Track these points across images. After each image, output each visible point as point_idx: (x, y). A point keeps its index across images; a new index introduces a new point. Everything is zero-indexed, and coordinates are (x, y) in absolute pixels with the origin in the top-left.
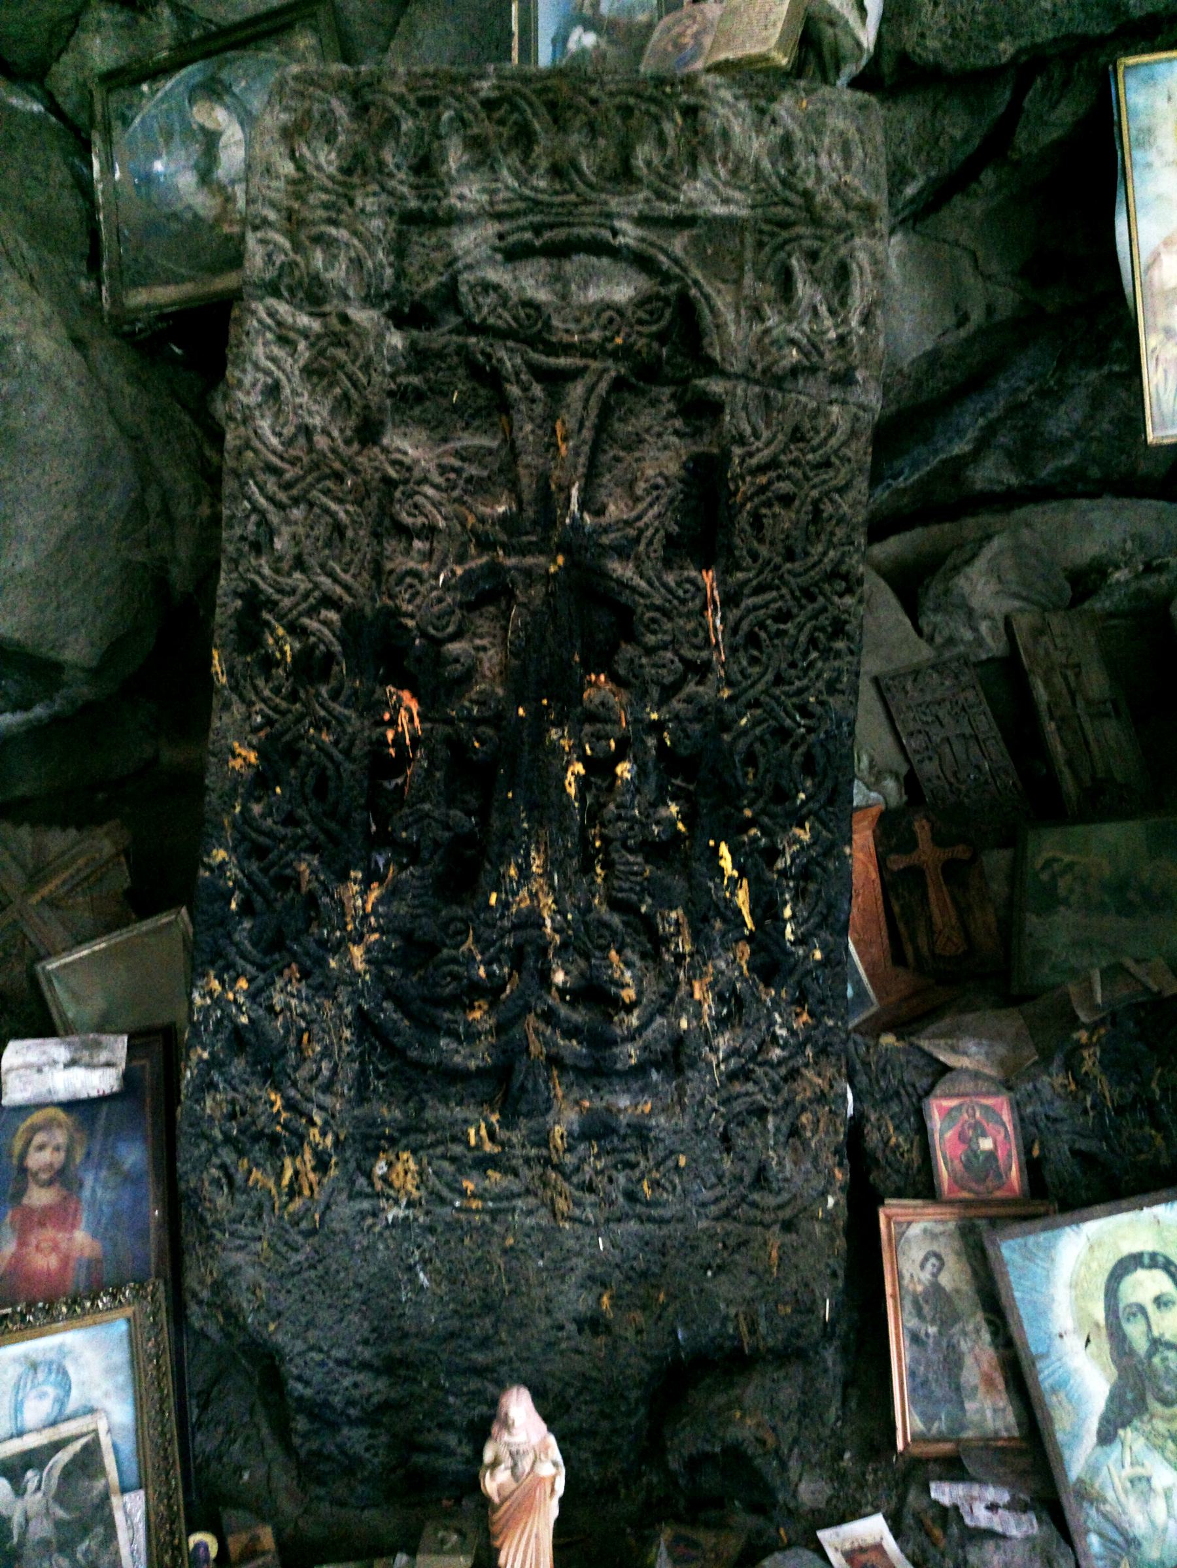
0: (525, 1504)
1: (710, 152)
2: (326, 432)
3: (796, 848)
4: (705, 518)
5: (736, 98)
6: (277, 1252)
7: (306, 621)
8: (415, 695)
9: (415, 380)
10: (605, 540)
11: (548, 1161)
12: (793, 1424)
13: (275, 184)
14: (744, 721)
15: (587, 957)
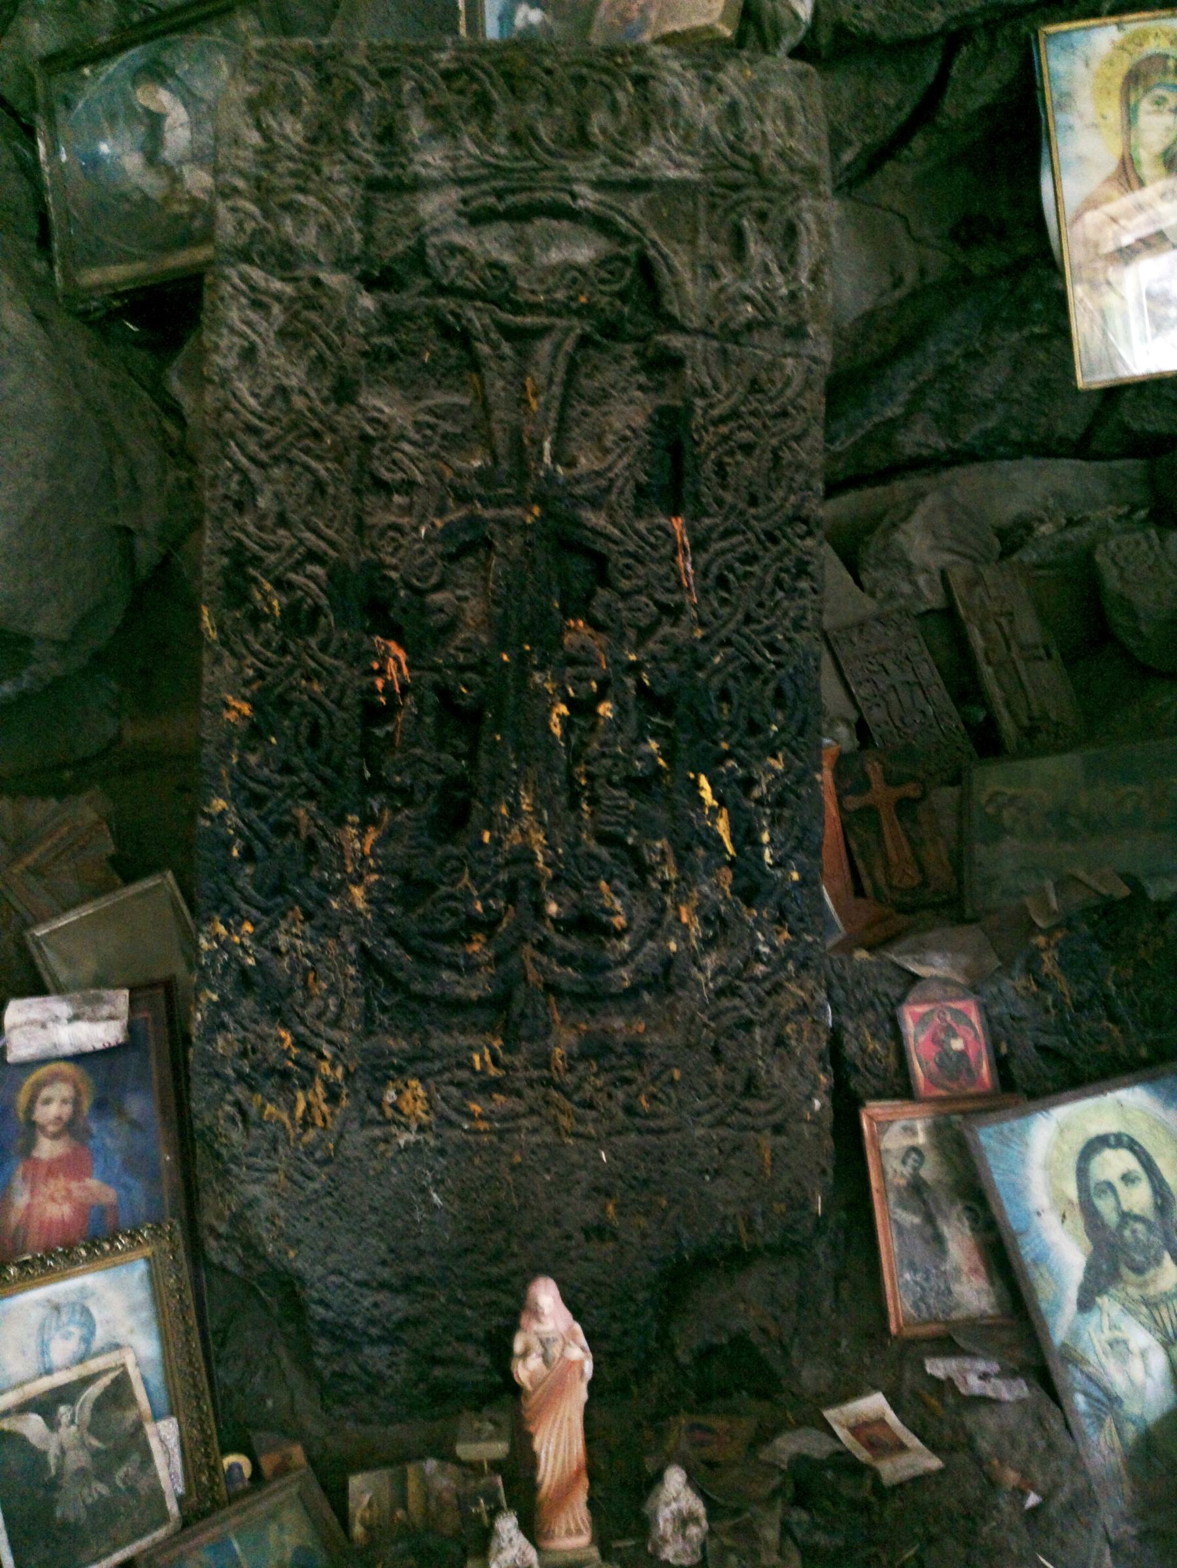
0: (556, 1388)
1: (661, 119)
2: (303, 392)
3: (771, 777)
4: (673, 468)
5: (684, 67)
6: (294, 1182)
7: (292, 576)
8: (401, 644)
9: (388, 340)
10: (578, 491)
11: (549, 1083)
12: (793, 1315)
13: (241, 153)
14: (717, 660)
15: (577, 888)
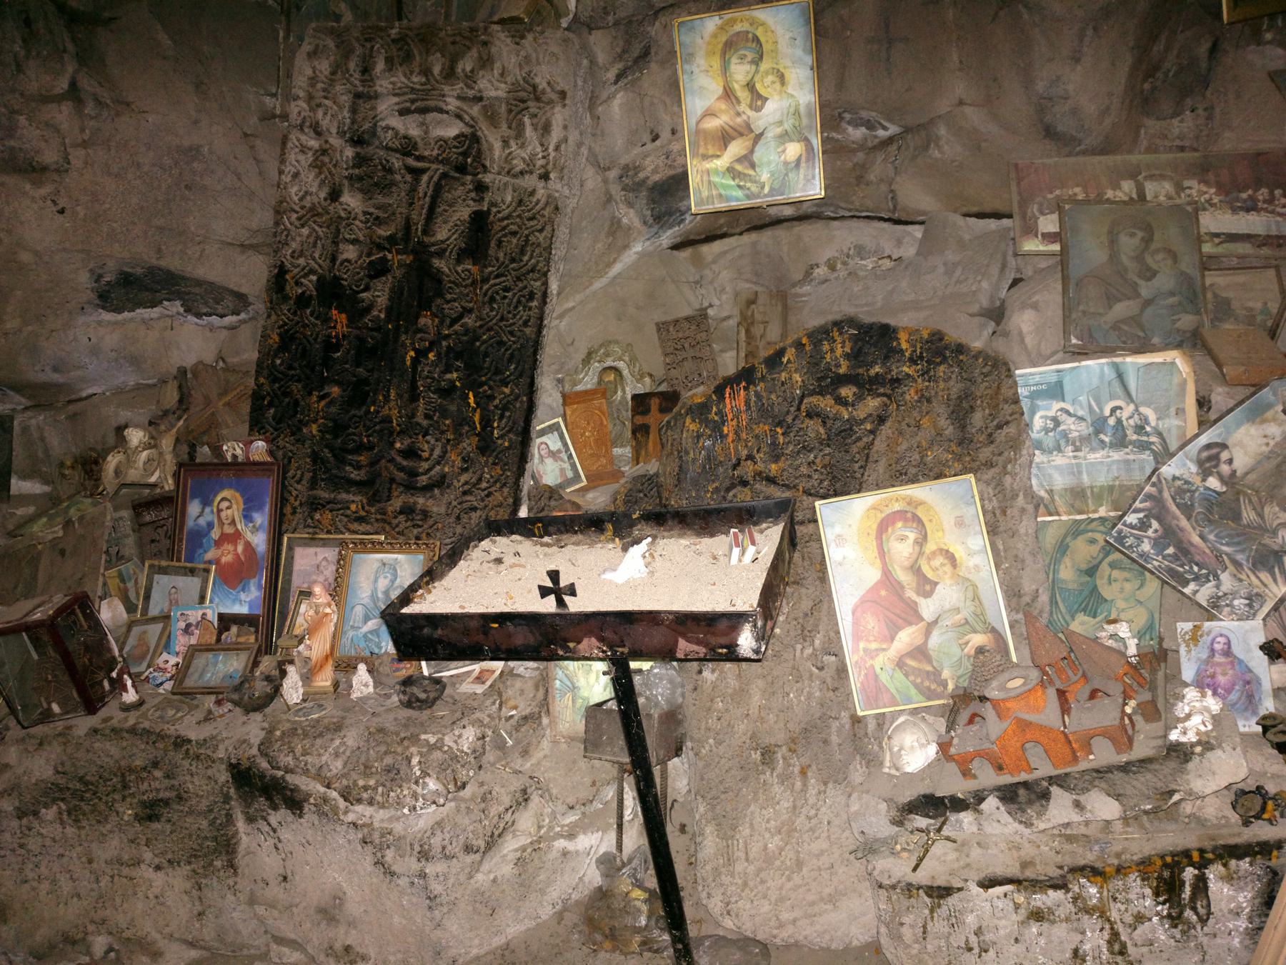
9: (357, 171)
10: (432, 249)
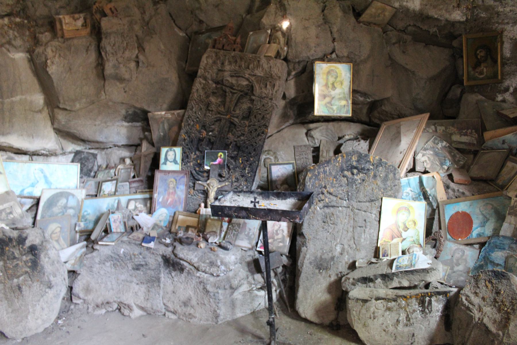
4: (248, 115)
